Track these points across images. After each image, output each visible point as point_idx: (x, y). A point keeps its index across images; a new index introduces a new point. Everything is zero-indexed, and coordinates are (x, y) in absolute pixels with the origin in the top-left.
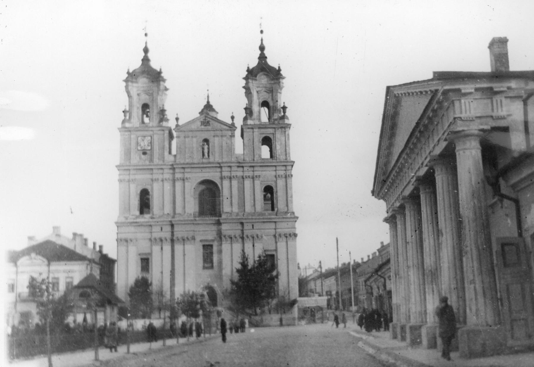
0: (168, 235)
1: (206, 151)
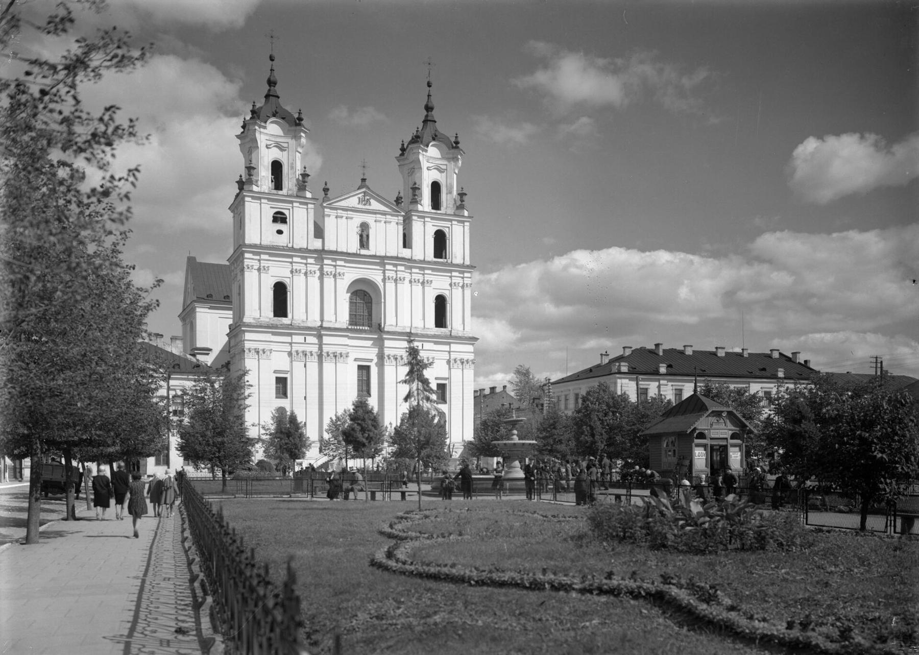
0: (315, 349)
1: (365, 239)
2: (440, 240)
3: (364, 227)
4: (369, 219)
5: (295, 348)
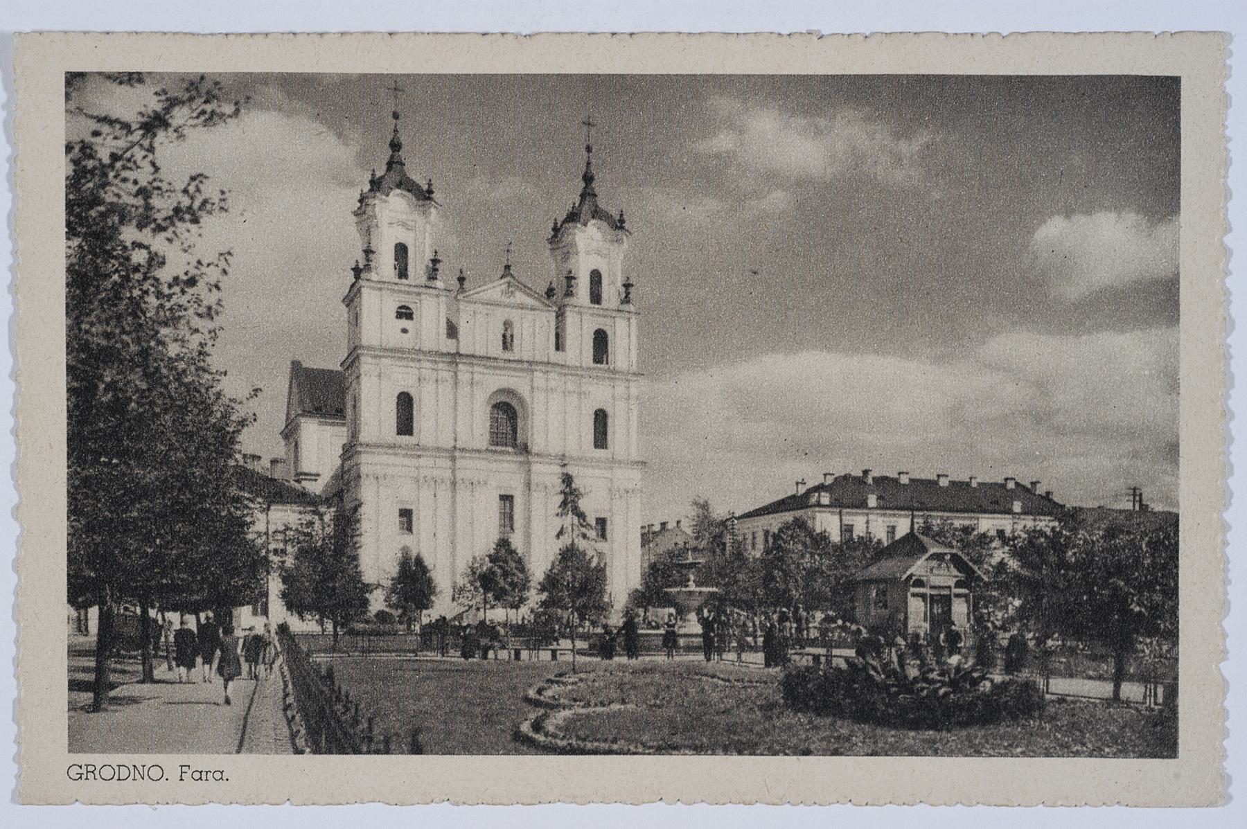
0: (448, 474)
2: (601, 341)
3: (507, 324)
4: (514, 315)
5: (423, 472)
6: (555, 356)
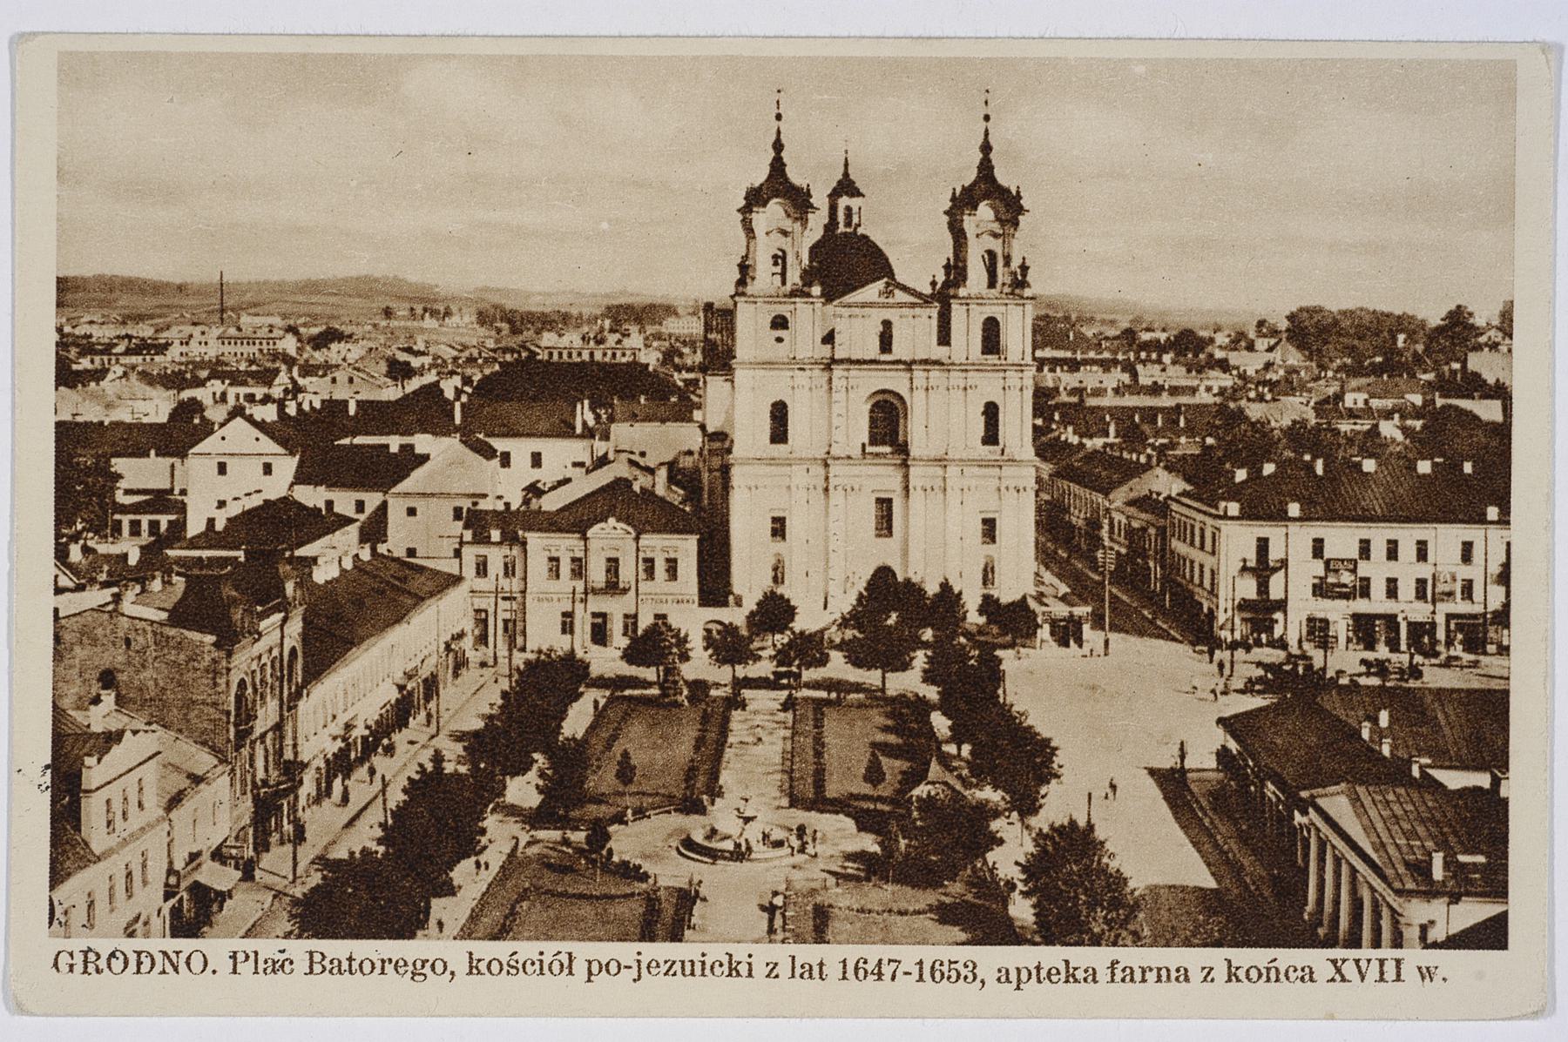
2: (991, 330)
3: (887, 324)
6: (940, 353)
